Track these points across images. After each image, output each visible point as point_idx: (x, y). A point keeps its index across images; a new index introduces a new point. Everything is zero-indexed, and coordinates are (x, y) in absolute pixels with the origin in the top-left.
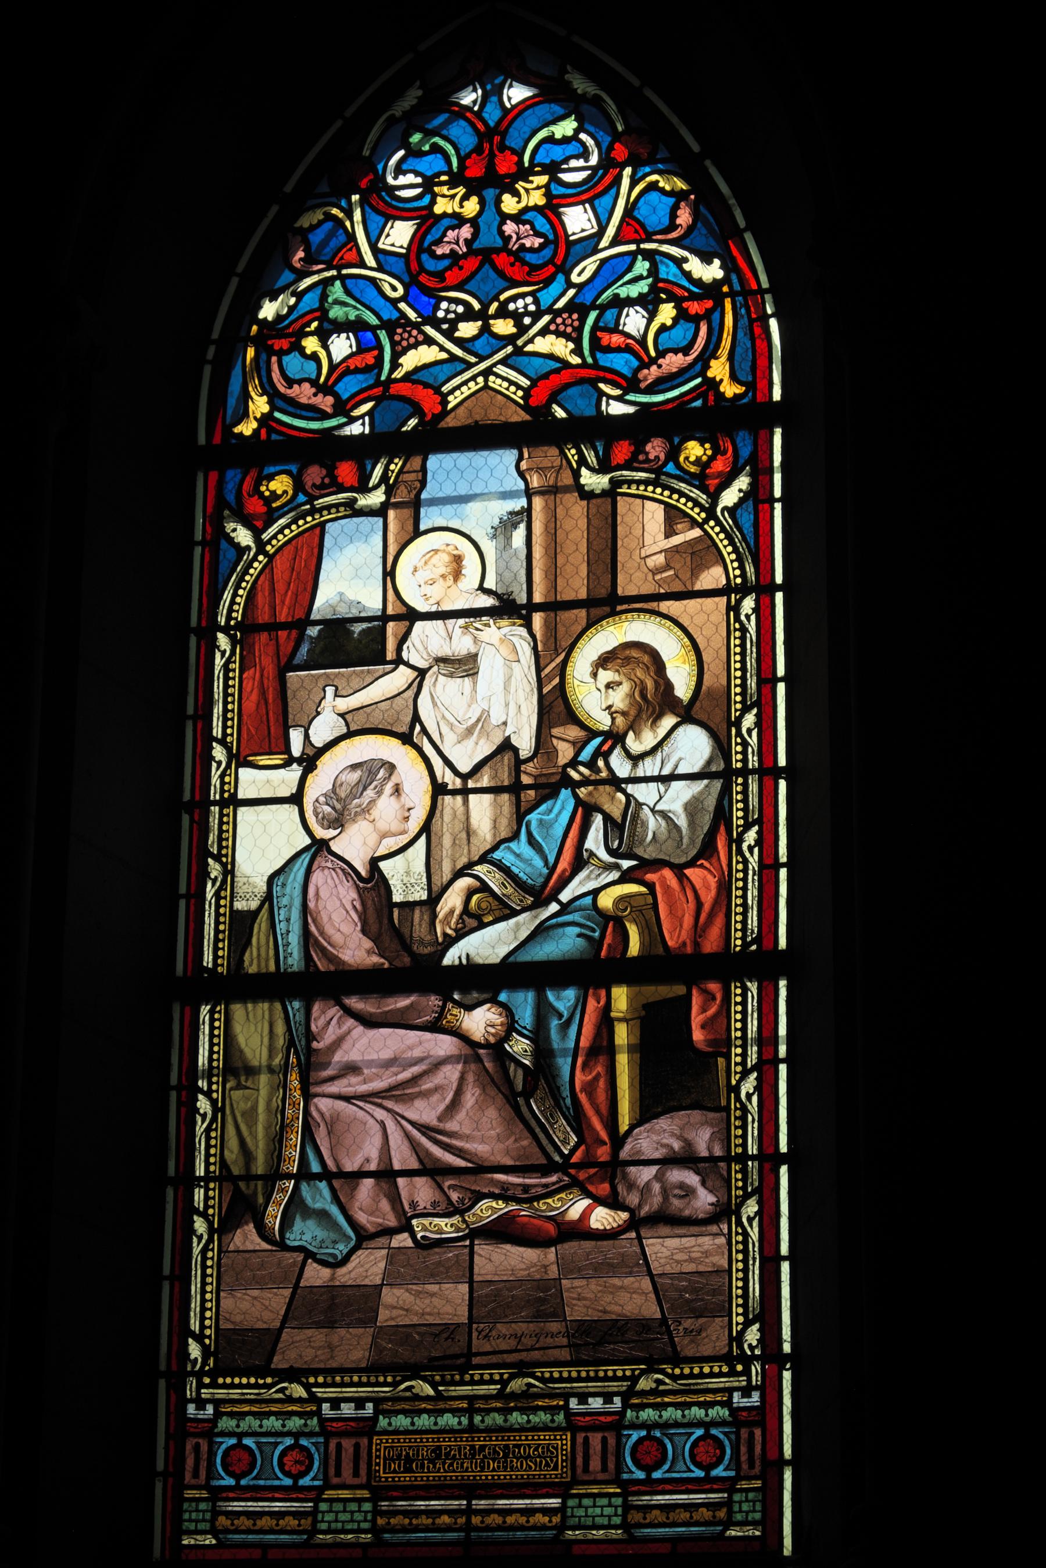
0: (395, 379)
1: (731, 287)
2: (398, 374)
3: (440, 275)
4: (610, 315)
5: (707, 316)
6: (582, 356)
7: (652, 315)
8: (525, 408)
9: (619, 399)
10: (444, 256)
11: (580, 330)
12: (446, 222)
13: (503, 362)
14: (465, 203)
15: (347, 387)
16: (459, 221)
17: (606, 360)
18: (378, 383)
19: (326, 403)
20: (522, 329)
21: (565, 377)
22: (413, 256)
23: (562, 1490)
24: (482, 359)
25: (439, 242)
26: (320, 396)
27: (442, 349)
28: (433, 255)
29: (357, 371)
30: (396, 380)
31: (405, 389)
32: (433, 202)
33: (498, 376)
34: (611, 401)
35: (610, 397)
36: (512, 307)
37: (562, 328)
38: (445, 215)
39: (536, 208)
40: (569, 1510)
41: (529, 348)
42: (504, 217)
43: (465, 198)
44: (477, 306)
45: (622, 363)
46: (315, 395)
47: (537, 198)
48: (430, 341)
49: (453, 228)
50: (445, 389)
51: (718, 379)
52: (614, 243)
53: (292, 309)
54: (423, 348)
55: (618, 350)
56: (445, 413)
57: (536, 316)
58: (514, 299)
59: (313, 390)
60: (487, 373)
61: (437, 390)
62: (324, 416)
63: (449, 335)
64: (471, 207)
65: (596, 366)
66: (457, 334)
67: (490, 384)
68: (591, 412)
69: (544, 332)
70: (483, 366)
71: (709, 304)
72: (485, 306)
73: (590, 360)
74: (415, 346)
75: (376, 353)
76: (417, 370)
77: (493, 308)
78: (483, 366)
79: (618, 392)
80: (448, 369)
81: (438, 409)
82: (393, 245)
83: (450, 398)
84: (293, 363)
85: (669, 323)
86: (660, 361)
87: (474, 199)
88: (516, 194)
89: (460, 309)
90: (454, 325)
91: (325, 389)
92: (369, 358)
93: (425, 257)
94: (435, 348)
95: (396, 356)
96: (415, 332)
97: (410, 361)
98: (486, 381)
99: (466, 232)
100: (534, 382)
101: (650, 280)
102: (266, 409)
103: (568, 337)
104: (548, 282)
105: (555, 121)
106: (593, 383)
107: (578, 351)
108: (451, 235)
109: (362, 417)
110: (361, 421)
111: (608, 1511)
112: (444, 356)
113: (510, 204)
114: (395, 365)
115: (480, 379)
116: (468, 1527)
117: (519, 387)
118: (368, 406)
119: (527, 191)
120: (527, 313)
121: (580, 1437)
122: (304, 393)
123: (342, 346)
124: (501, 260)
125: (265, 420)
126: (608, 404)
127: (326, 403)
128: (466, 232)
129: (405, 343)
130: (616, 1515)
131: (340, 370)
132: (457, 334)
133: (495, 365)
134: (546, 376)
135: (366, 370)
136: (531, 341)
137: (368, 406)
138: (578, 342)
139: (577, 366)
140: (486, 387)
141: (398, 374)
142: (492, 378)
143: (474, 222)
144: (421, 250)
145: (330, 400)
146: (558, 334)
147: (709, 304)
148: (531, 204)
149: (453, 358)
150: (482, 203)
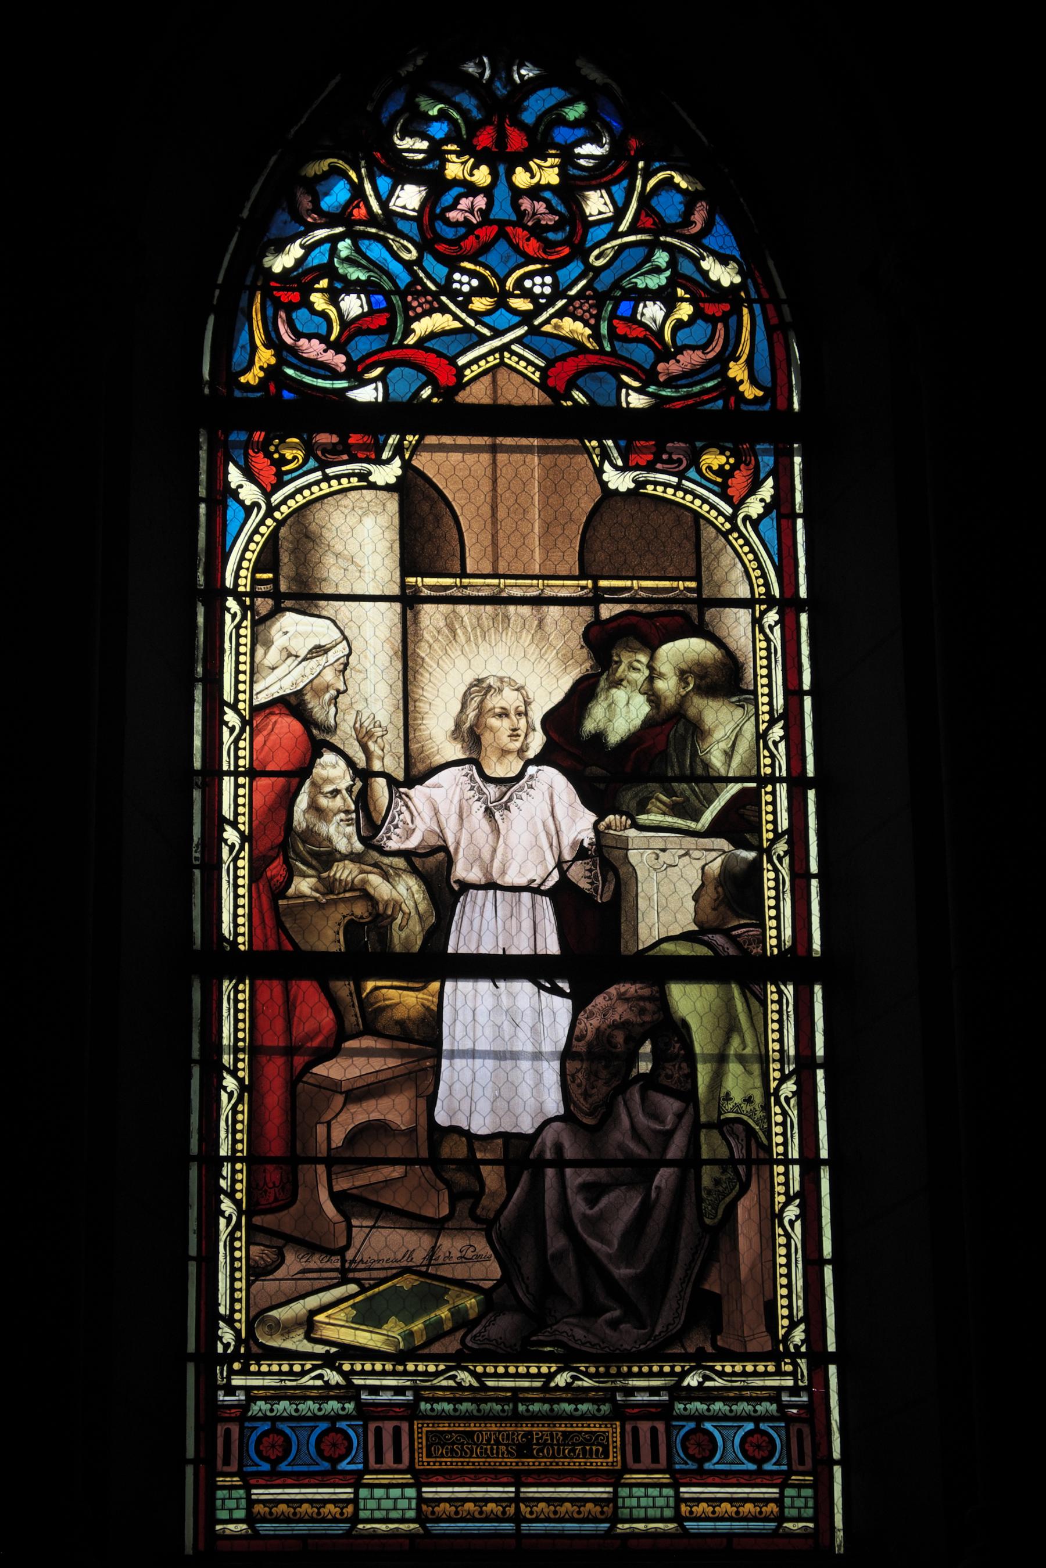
0: (407, 345)
1: (747, 293)
2: (411, 340)
3: (456, 242)
4: (625, 308)
5: (724, 318)
6: (600, 343)
7: (670, 309)
8: (542, 386)
9: (639, 391)
10: (457, 224)
11: (598, 318)
12: (456, 191)
13: (518, 340)
14: (475, 172)
15: (363, 345)
16: (471, 189)
17: (623, 349)
18: (389, 347)
19: (339, 361)
20: (539, 310)
21: (582, 362)
22: (426, 220)
23: (614, 1478)
24: (498, 333)
25: (453, 207)
26: (331, 352)
27: (456, 318)
28: (448, 222)
29: (368, 332)
30: (408, 346)
31: (420, 356)
32: (442, 168)
33: (513, 353)
34: (630, 392)
35: (628, 387)
36: (528, 284)
37: (579, 312)
38: (456, 182)
39: (548, 187)
40: (620, 1501)
41: (547, 328)
42: (517, 193)
43: (475, 166)
44: (493, 281)
45: (642, 354)
46: (325, 351)
47: (551, 176)
48: (444, 310)
49: (466, 195)
50: (461, 361)
51: (738, 380)
52: (630, 231)
53: (300, 262)
54: (437, 316)
55: (636, 340)
56: (461, 386)
57: (551, 300)
58: (530, 275)
59: (323, 346)
60: (506, 347)
61: (452, 360)
62: (335, 375)
63: (464, 306)
64: (482, 176)
65: (613, 353)
66: (470, 306)
67: (506, 360)
68: (612, 403)
69: (560, 314)
70: (496, 343)
71: (726, 307)
72: (502, 282)
73: (608, 349)
74: (429, 313)
75: (388, 315)
76: (433, 335)
77: (510, 283)
78: (496, 343)
79: (636, 384)
80: (464, 339)
81: (452, 381)
82: (404, 207)
83: (467, 372)
84: (301, 316)
85: (686, 318)
86: (679, 357)
87: (484, 169)
88: (528, 169)
89: (475, 283)
90: (468, 297)
91: (338, 347)
92: (382, 320)
93: (439, 225)
94: (448, 317)
95: (409, 321)
96: (429, 298)
97: (423, 327)
98: (502, 357)
99: (481, 202)
100: (551, 363)
101: (668, 273)
102: (273, 361)
103: (586, 324)
104: (564, 262)
105: (570, 102)
106: (615, 373)
107: (596, 336)
108: (465, 203)
109: (374, 380)
110: (374, 385)
111: (661, 1502)
112: (457, 325)
113: (521, 178)
114: (408, 332)
115: (497, 355)
116: (518, 1519)
117: (537, 367)
118: (378, 371)
119: (540, 167)
120: (542, 295)
121: (628, 1427)
122: (313, 349)
123: (353, 305)
124: (519, 235)
125: (272, 373)
126: (628, 395)
127: (339, 361)
128: (481, 202)
129: (419, 310)
130: (668, 1507)
131: (352, 328)
132: (470, 306)
133: (512, 342)
134: (563, 358)
135: (378, 332)
136: (547, 321)
137: (378, 371)
138: (595, 329)
139: (593, 352)
140: (502, 363)
141: (411, 340)
142: (506, 354)
143: (488, 191)
144: (433, 217)
145: (342, 358)
146: (575, 318)
147: (726, 307)
148: (543, 182)
149: (466, 329)
150: (494, 173)
